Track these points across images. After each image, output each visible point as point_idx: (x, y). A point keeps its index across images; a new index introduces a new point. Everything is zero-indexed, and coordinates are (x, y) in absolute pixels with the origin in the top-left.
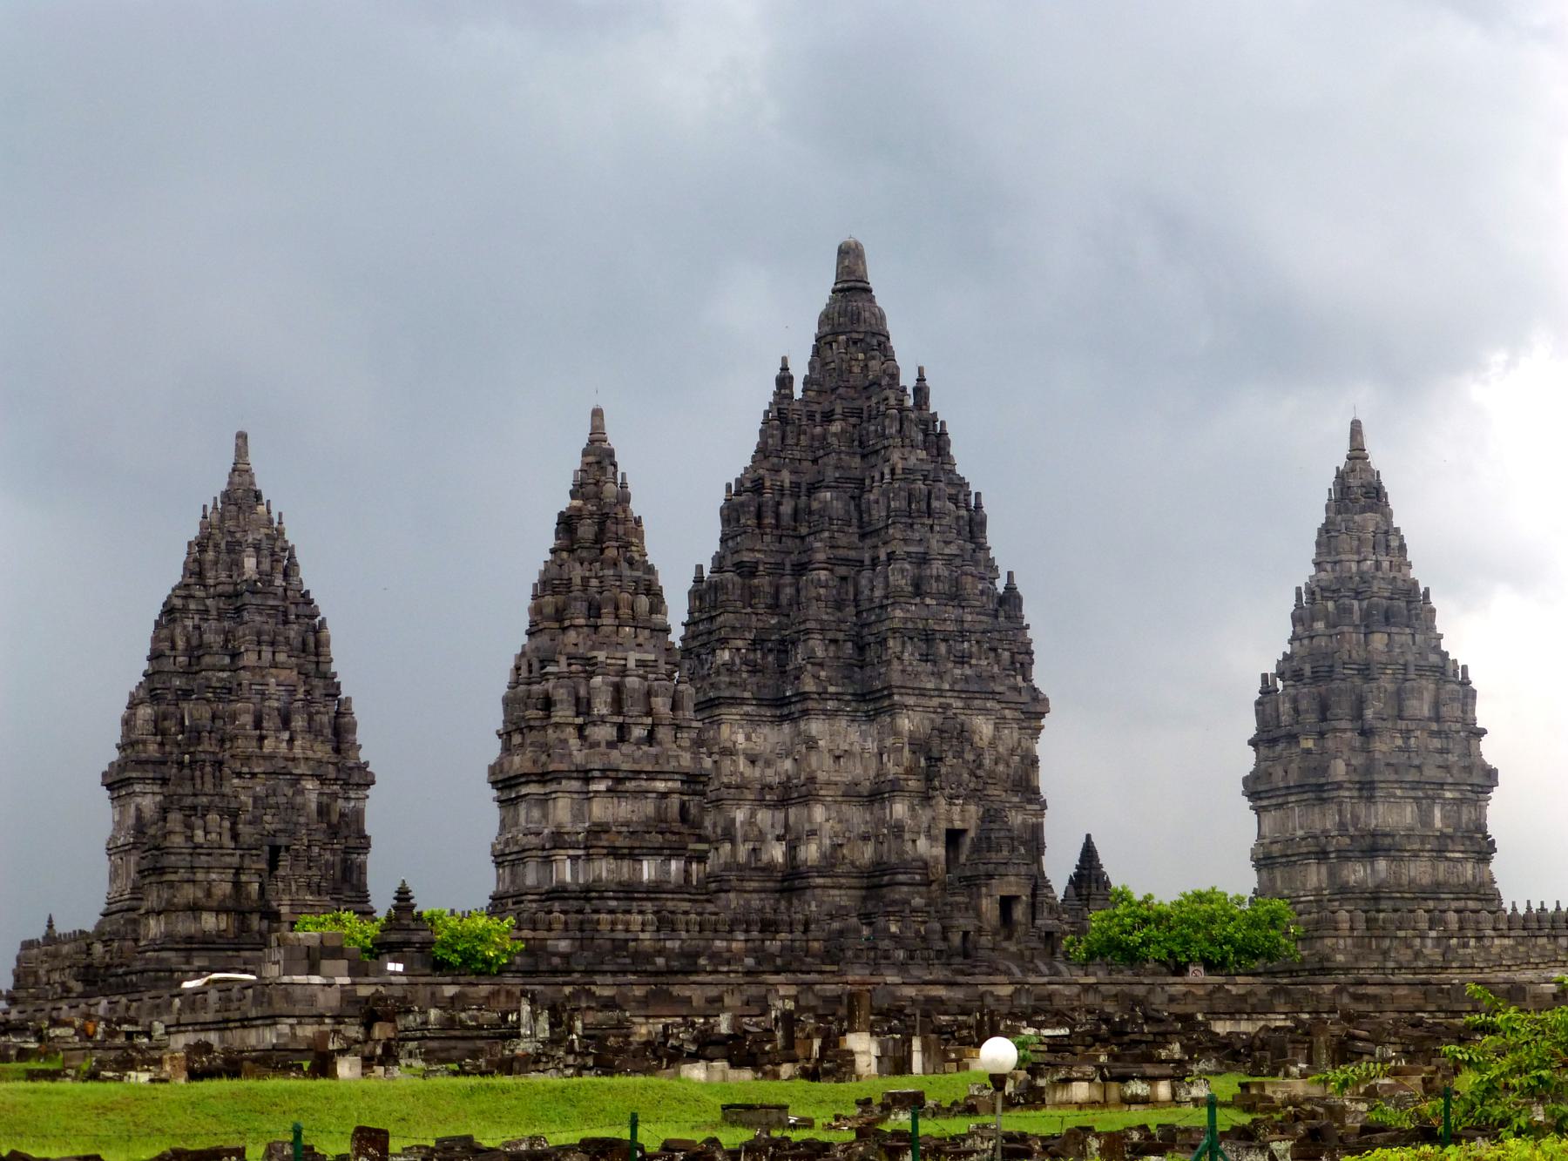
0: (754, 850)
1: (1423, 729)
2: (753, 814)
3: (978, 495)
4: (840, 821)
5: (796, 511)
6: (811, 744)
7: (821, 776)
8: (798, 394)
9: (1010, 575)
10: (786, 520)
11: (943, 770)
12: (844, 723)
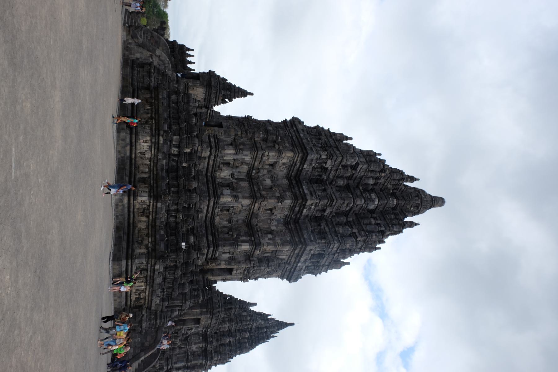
0: (229, 164)
2: (247, 164)
4: (240, 211)
6: (281, 199)
7: (264, 203)
11: (263, 268)
12: (286, 213)
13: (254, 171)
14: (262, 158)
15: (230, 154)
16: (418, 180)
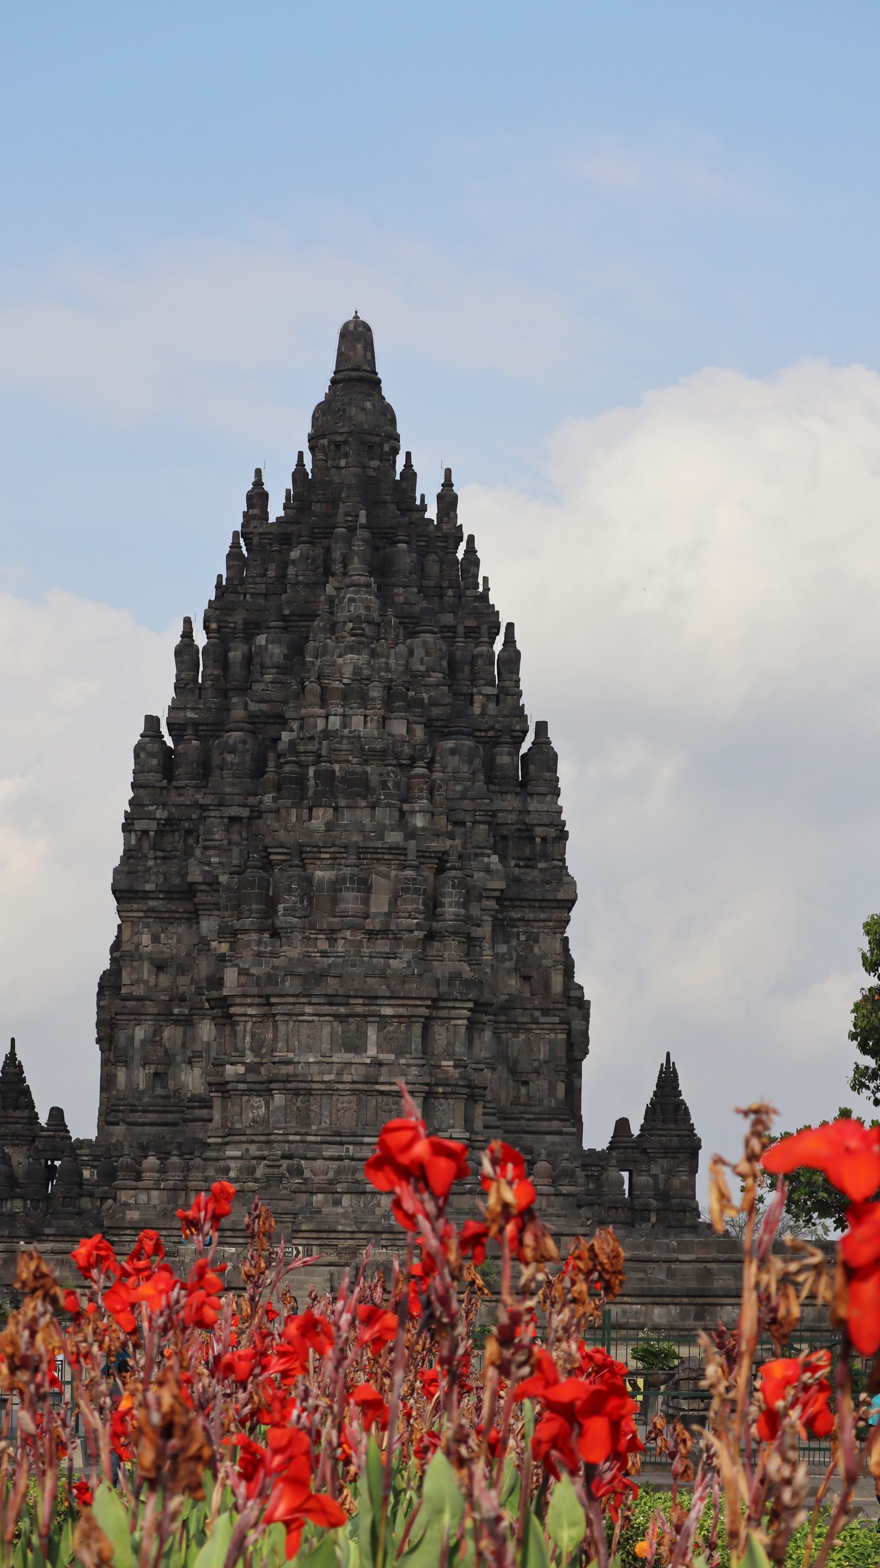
0: (157, 1075)
1: (353, 928)
3: (510, 626)
5: (249, 659)
8: (276, 510)
9: (542, 727)
10: (236, 670)
13: (176, 1011)
14: (139, 999)
15: (129, 1077)
16: (258, 472)
